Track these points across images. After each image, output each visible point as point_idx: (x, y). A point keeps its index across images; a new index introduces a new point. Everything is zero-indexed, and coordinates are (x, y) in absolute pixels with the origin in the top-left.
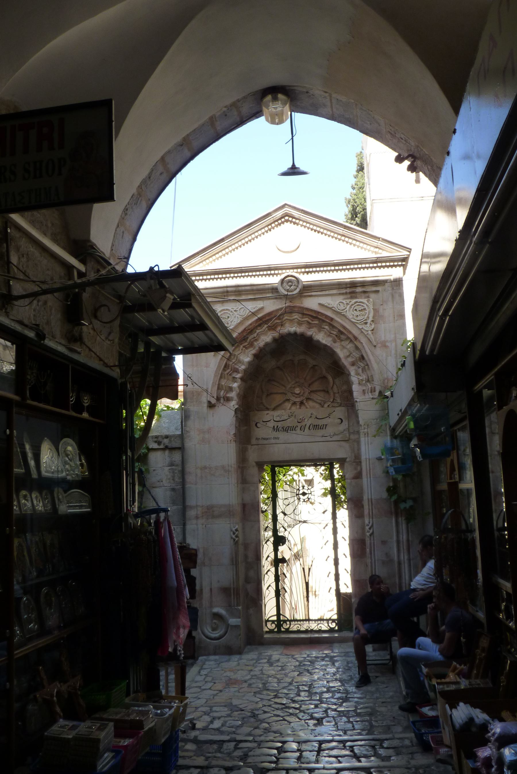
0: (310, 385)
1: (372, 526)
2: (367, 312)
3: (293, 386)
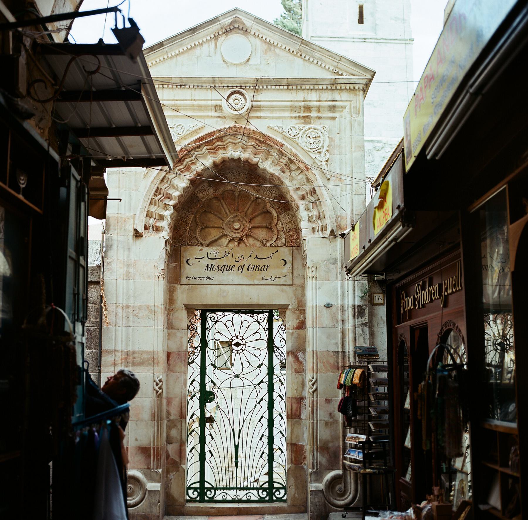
0: (251, 220)
1: (316, 381)
2: (322, 140)
3: (232, 220)
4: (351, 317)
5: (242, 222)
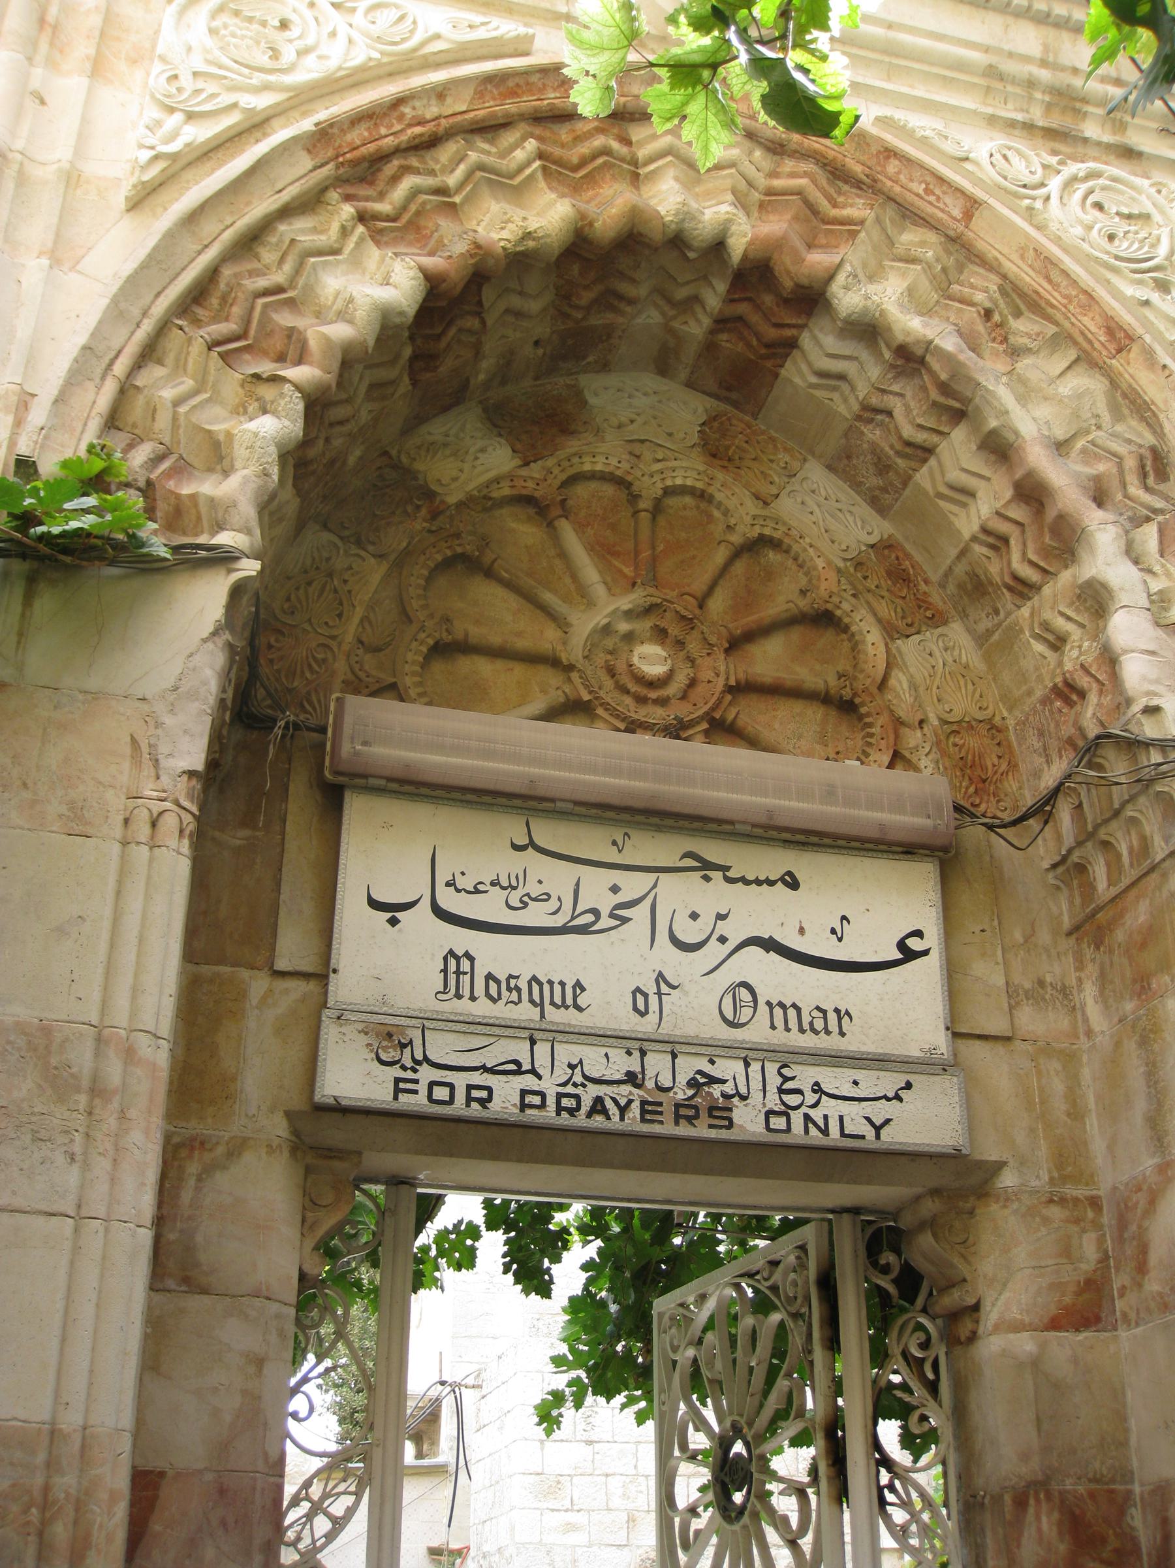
3: (624, 627)
5: (680, 644)
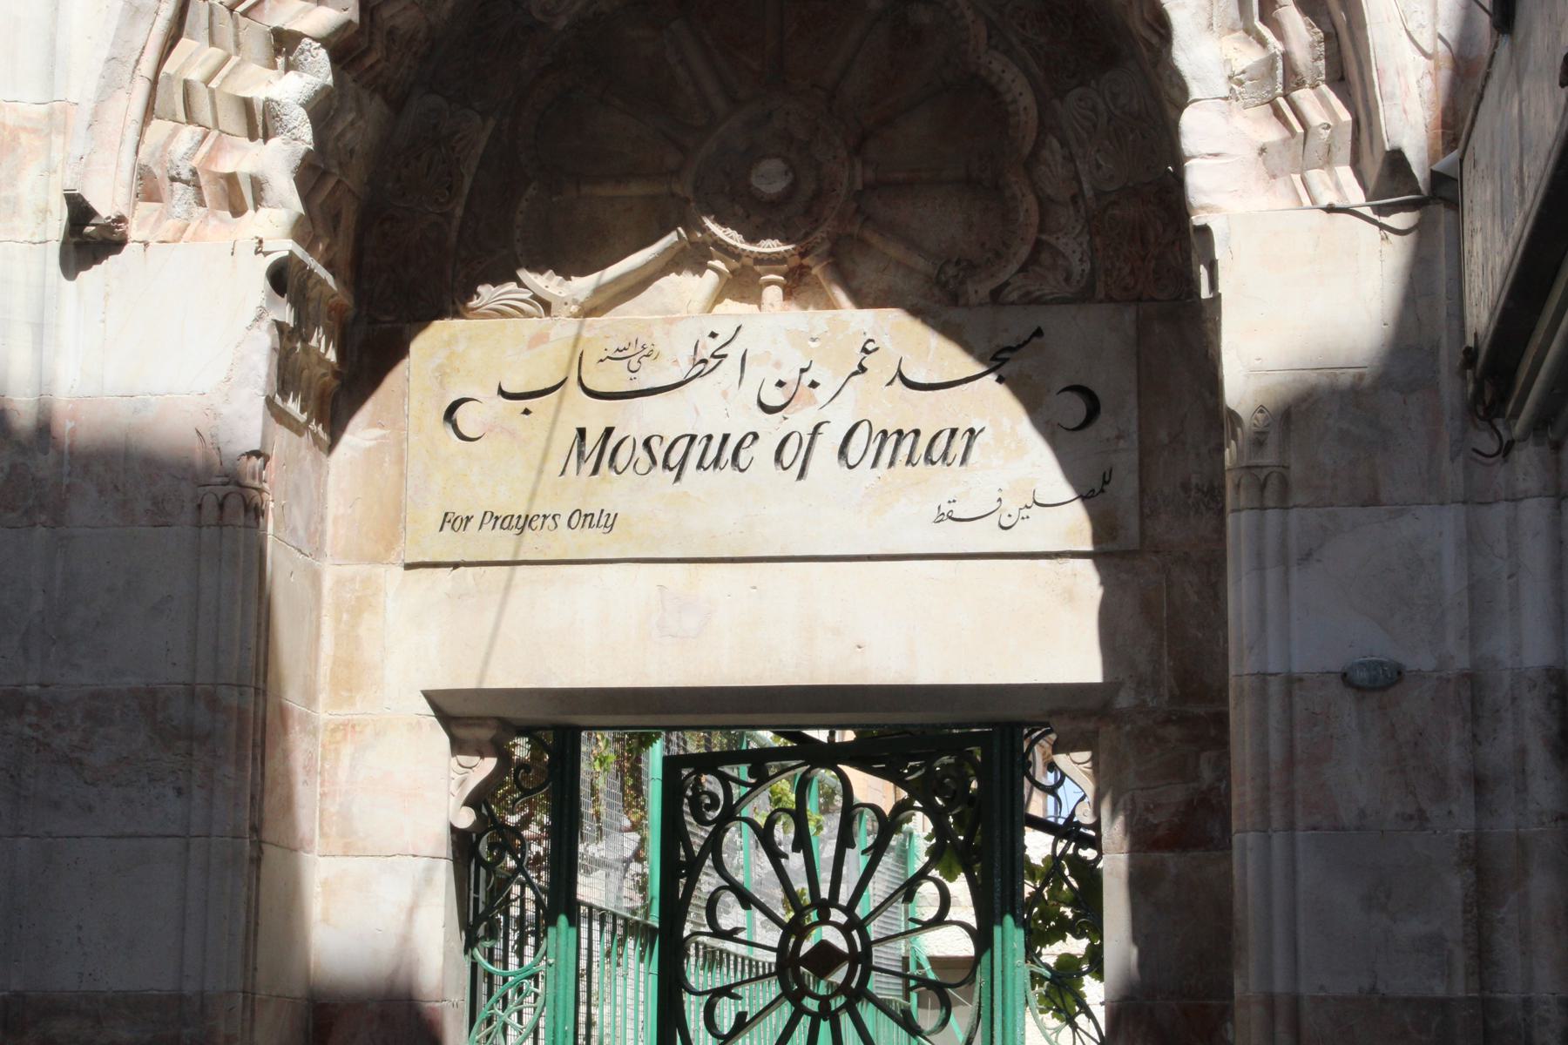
4: (1538, 756)
